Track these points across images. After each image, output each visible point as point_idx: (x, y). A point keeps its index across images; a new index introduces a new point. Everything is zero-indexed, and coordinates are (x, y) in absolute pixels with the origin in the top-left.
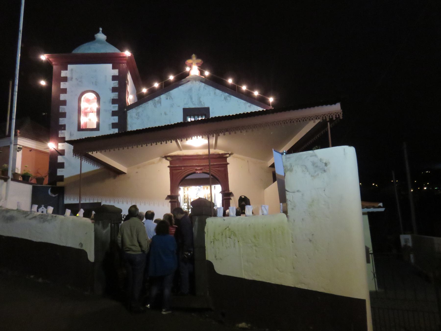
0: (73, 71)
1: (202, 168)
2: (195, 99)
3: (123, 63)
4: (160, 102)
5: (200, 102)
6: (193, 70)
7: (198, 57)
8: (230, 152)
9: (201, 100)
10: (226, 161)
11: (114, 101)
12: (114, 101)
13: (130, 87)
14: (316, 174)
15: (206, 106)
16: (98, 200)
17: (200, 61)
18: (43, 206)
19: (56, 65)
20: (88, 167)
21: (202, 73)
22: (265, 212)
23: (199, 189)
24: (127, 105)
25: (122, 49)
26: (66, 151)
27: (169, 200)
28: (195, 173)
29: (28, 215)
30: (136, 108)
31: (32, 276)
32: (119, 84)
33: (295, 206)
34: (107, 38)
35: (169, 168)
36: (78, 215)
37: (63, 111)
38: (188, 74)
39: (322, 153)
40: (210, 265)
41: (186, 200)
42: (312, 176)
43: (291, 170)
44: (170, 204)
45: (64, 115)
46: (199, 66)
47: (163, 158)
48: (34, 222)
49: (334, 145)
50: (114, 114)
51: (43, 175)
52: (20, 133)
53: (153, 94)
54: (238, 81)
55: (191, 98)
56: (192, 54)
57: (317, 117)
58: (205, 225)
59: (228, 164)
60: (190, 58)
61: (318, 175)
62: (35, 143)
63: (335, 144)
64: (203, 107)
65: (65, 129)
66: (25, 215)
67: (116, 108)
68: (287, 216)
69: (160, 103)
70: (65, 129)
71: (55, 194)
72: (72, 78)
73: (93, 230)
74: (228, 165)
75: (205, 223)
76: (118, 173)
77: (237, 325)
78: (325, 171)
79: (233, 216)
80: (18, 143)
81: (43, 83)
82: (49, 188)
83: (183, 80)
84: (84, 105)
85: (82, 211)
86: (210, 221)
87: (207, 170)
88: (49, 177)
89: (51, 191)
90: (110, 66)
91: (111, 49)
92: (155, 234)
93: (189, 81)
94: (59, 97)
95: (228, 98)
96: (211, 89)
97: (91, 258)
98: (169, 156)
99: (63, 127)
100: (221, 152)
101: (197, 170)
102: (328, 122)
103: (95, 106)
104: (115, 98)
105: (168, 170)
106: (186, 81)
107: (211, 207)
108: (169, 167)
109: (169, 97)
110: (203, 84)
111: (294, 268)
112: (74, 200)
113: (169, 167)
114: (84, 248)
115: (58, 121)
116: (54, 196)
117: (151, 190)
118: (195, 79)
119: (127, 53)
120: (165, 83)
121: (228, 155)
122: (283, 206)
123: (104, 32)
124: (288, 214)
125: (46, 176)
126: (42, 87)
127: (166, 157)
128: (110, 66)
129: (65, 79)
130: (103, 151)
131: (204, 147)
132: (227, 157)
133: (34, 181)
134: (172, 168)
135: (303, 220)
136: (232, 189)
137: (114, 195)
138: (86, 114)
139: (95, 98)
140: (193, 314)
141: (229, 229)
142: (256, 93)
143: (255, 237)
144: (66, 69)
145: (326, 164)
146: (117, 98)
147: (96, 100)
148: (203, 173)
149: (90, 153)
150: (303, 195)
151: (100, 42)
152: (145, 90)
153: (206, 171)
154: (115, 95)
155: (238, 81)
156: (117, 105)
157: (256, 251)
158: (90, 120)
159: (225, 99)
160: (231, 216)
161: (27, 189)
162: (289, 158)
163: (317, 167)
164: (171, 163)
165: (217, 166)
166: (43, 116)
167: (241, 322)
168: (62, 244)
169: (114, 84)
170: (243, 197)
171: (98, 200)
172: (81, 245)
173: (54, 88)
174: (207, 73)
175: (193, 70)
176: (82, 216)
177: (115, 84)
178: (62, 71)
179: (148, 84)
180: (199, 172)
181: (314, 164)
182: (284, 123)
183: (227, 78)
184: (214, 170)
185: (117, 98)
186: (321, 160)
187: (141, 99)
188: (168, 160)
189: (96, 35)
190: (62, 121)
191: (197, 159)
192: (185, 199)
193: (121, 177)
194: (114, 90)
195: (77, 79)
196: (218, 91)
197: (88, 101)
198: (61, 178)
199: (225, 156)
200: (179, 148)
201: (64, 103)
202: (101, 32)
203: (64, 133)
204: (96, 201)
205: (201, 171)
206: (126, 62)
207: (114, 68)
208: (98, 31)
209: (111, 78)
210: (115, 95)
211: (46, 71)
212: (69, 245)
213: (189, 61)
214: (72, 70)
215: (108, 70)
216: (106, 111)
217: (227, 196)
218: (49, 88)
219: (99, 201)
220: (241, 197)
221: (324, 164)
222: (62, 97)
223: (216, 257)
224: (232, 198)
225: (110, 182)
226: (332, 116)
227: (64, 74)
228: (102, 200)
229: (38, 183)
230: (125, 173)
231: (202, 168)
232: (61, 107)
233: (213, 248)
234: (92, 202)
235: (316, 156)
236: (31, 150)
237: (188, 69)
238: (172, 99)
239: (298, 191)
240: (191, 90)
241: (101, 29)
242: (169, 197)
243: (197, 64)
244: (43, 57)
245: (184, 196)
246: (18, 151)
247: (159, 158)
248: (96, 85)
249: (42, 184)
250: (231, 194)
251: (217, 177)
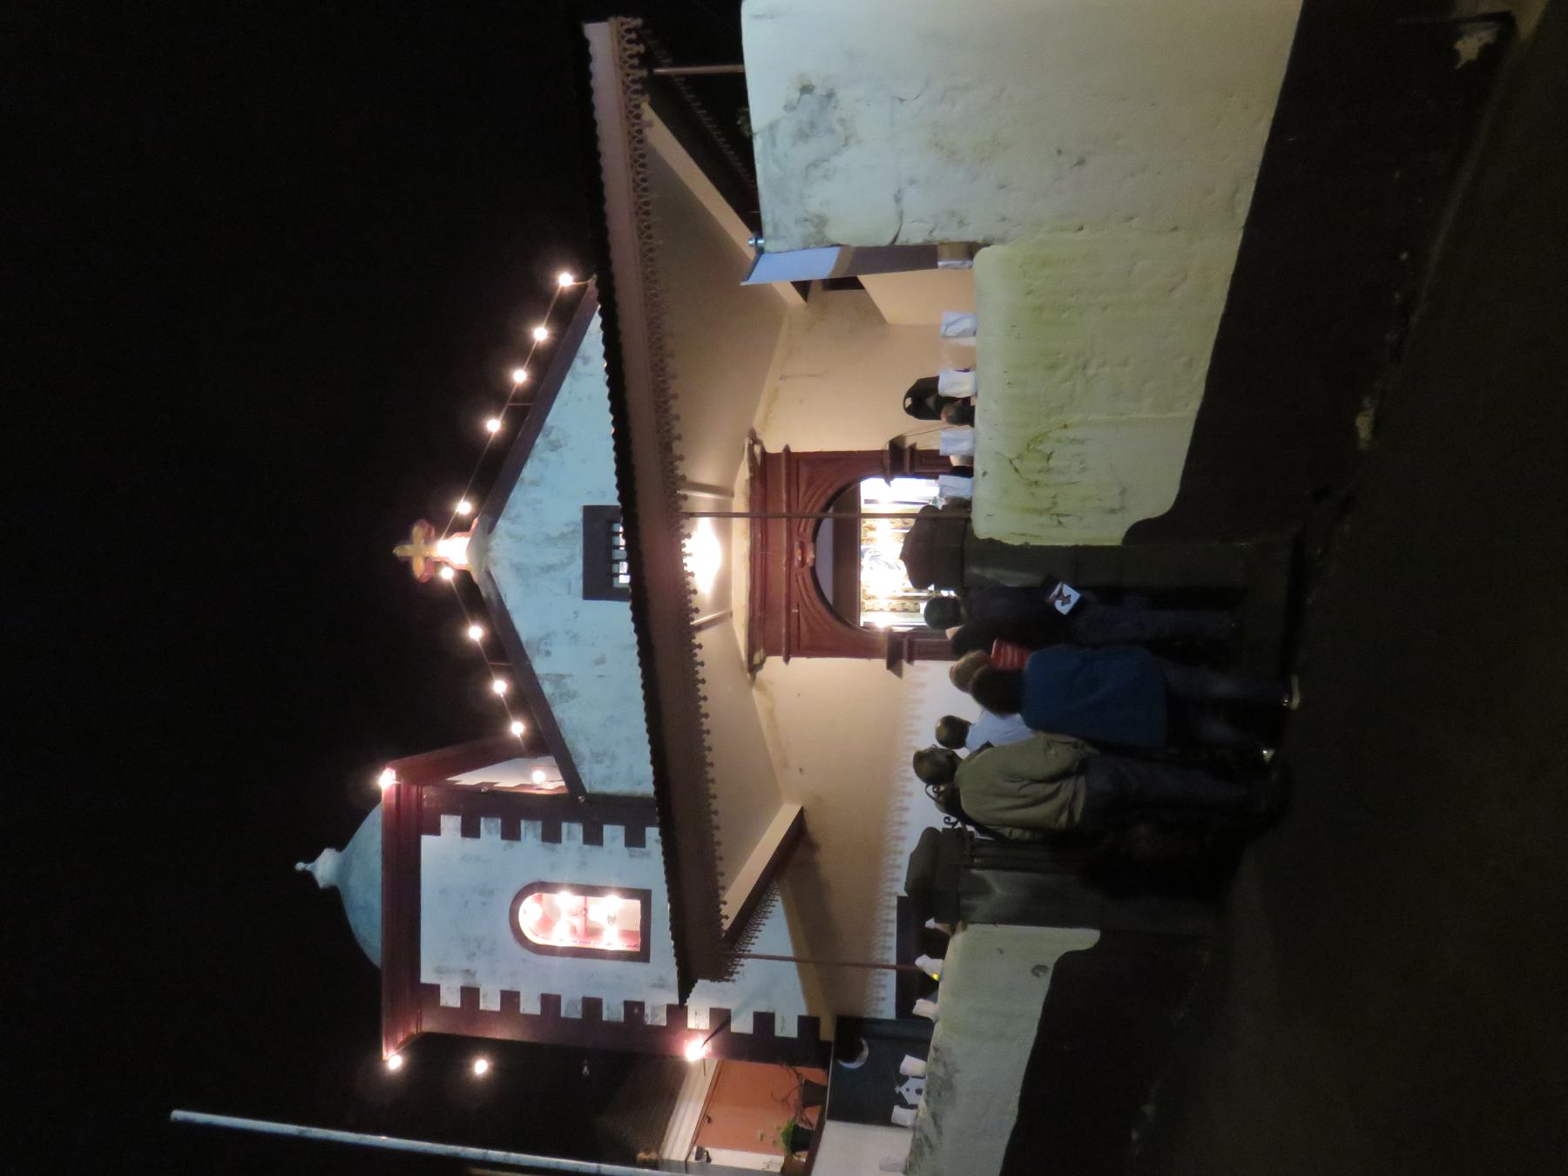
0: (441, 965)
1: (796, 544)
2: (553, 555)
3: (420, 796)
4: (559, 678)
5: (563, 536)
6: (449, 555)
7: (406, 537)
8: (747, 442)
9: (555, 533)
10: (777, 456)
11: (551, 836)
12: (551, 836)
13: (503, 778)
14: (838, 128)
15: (579, 516)
16: (889, 907)
17: (418, 531)
18: (898, 1089)
19: (419, 1021)
20: (774, 933)
21: (462, 526)
22: (967, 324)
23: (873, 558)
24: (565, 791)
25: (375, 798)
26: (716, 1005)
27: (905, 664)
28: (813, 570)
29: (926, 1138)
30: (575, 761)
31: (1135, 1136)
32: (490, 814)
33: (953, 214)
34: (330, 846)
35: (793, 660)
36: (935, 977)
37: (580, 1007)
38: (464, 576)
39: (766, 103)
40: (1141, 531)
41: (909, 604)
42: (846, 145)
43: (822, 222)
44: (917, 663)
45: (592, 1006)
46: (438, 535)
47: (754, 678)
48: (951, 1121)
49: (737, 55)
50: (593, 837)
51: (795, 1082)
52: (647, 1151)
53: (529, 698)
54: (497, 396)
55: (549, 568)
56: (395, 558)
57: (633, 115)
58: (999, 543)
59: (787, 449)
60: (406, 565)
61: (842, 121)
62: (684, 1104)
63: (735, 52)
64: (581, 528)
65: (641, 1005)
66: (926, 1150)
67: (573, 831)
68: (988, 245)
69: (562, 676)
70: (641, 1005)
71: (862, 1049)
72: (467, 972)
73: (990, 928)
74: (793, 450)
75: (991, 541)
76: (799, 834)
77: (1363, 446)
78: (830, 95)
79: (974, 442)
80: (683, 1158)
81: (481, 1067)
82: (839, 1063)
83: (484, 594)
84: (561, 937)
85: (924, 962)
86: (984, 526)
87: (807, 527)
89: (851, 1059)
90: (427, 841)
91: (371, 835)
92: (1018, 716)
93: (489, 574)
94: (529, 1018)
95: (553, 436)
96: (520, 498)
97: (1084, 938)
98: (750, 657)
99: (634, 1009)
100: (744, 473)
101: (803, 562)
102: (651, 72)
103: (566, 900)
104: (540, 831)
105: (798, 662)
106: (489, 583)
107: (935, 519)
108: (787, 660)
109: (542, 647)
110: (501, 523)
111: (1175, 229)
112: (884, 987)
113: (787, 660)
114: (1050, 962)
115: (611, 1025)
116: (866, 1053)
117: (861, 721)
118: (480, 549)
119: (387, 780)
120: (491, 659)
121: (757, 449)
122: (952, 257)
123: (312, 857)
124: (980, 239)
125: (799, 1075)
126: (498, 1070)
127: (753, 668)
128: (427, 841)
129: (470, 995)
130: (721, 881)
131: (725, 533)
132: (764, 453)
133: (812, 1115)
134: (795, 647)
135: (1002, 187)
136: (879, 443)
137: (874, 853)
138: (592, 932)
139: (540, 899)
140: (1310, 601)
141: (1020, 457)
142: (541, 334)
143: (1053, 367)
144: (434, 990)
145: (806, 89)
146: (539, 824)
147: (545, 895)
148: (814, 539)
149: (726, 924)
150: (912, 182)
151: (344, 870)
152: (518, 728)
153: (810, 531)
154: (530, 831)
155: (497, 396)
156: (565, 826)
157: (1103, 365)
158: (612, 920)
159: (554, 447)
160: (973, 450)
161: (837, 1137)
162: (776, 227)
163: (813, 125)
164: (776, 653)
165: (794, 491)
166: (593, 1076)
167: (1352, 431)
168: (1033, 1033)
169: (489, 832)
170: (909, 402)
171: (889, 907)
172: (1038, 970)
173: (501, 1033)
174: (464, 507)
175: (449, 555)
176: (938, 962)
177: (490, 828)
178: (443, 1002)
179: (495, 715)
180: (810, 556)
181: (802, 135)
182: (650, 237)
183: (482, 437)
184: (807, 501)
185: (539, 824)
186: (790, 107)
187: (545, 741)
188: (763, 662)
189: (321, 884)
190: (613, 1011)
191: (765, 558)
192: (905, 610)
193: (812, 825)
194: (511, 833)
195: (471, 956)
196: (527, 472)
197: (546, 923)
198: (808, 1024)
199: (759, 459)
200: (723, 619)
201: (550, 1002)
202: (309, 867)
203: (654, 1008)
204: (894, 915)
205: (810, 547)
206: (414, 790)
207: (436, 831)
208: (308, 877)
209: (468, 840)
210: (530, 831)
211: (439, 1054)
212: (1036, 1009)
213: (419, 568)
214: (439, 971)
215: (442, 850)
216: (583, 865)
217: (900, 460)
218: (498, 1049)
219: (895, 902)
220: (909, 410)
221: (806, 97)
222: (530, 1006)
223: (1113, 511)
224: (909, 442)
225: (831, 862)
226: (631, 57)
227: (450, 998)
228: (890, 894)
230: (802, 812)
231: (796, 544)
232: (563, 1014)
233: (1081, 519)
234: (893, 928)
235: (772, 127)
236: (706, 1119)
237: (447, 575)
238: (548, 636)
239: (898, 200)
240: (518, 569)
241: (300, 866)
242: (894, 664)
243: (428, 540)
244: (394, 1061)
245: (893, 610)
246: (709, 1160)
247: (755, 692)
248: (491, 893)
249: (825, 1088)
250: (896, 446)
251: (830, 492)
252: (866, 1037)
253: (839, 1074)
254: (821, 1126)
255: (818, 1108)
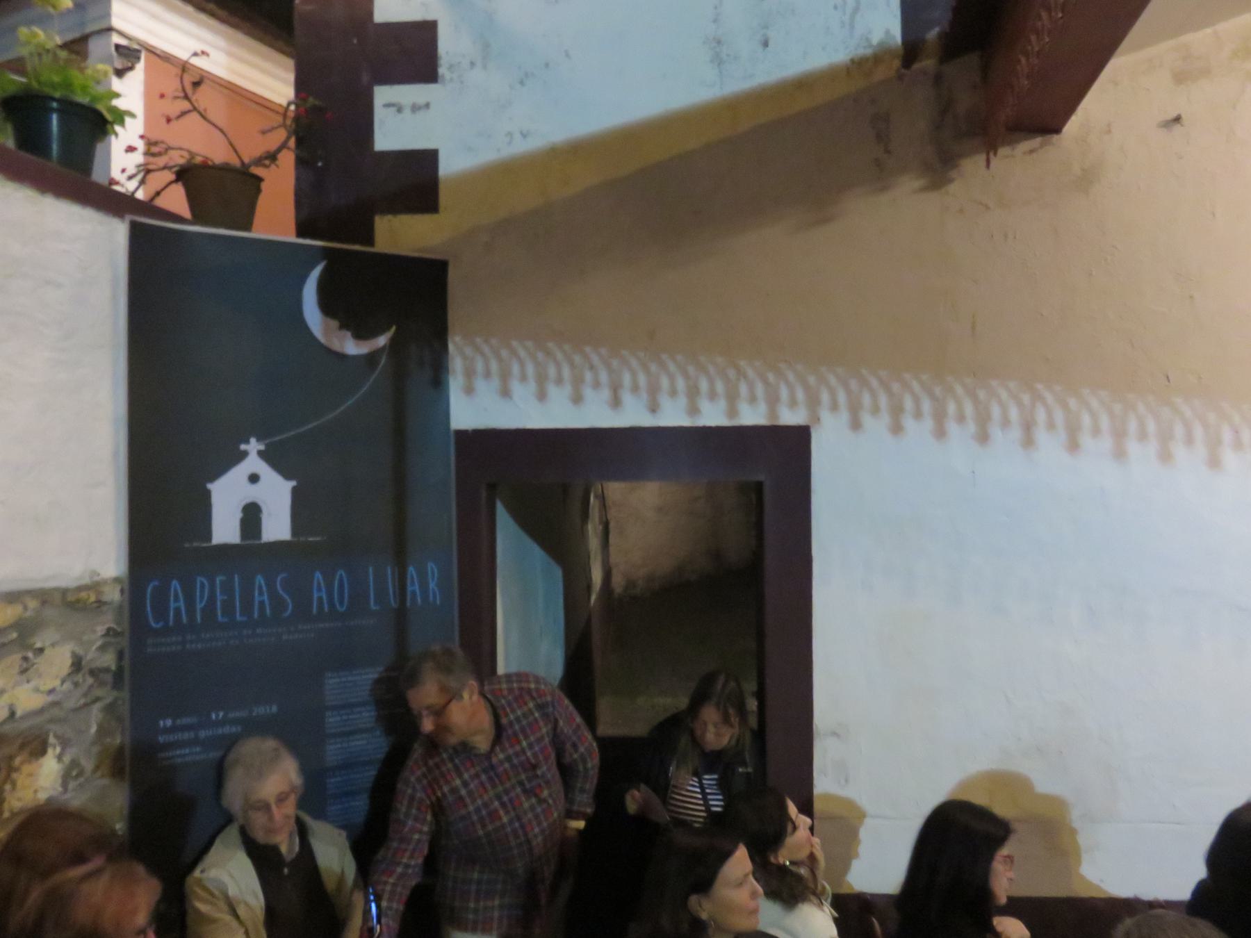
16: (773, 401)
18: (253, 446)
51: (251, 149)
71: (361, 334)
80: (116, 22)
88: (301, 162)
89: (328, 305)
125: (272, 157)
171: (773, 401)
198: (416, 181)
204: (752, 416)
219: (790, 417)
228: (813, 403)
229: (198, 218)
234: (713, 416)
246: (120, 73)
249: (248, 228)
252: (395, 346)
253: (284, 263)
254: (109, 201)
255: (187, 214)
